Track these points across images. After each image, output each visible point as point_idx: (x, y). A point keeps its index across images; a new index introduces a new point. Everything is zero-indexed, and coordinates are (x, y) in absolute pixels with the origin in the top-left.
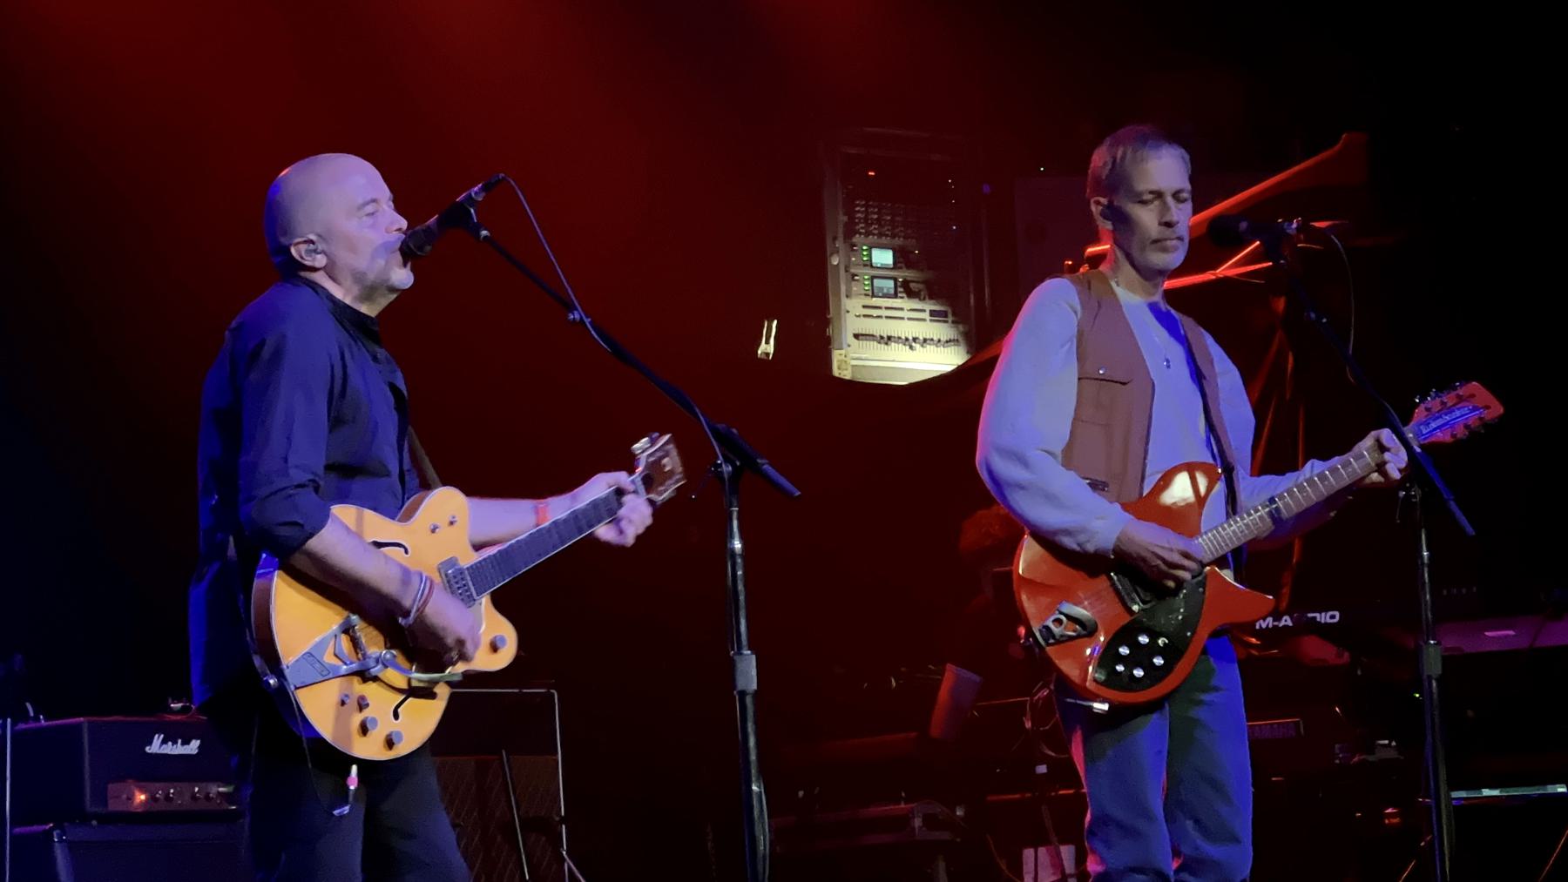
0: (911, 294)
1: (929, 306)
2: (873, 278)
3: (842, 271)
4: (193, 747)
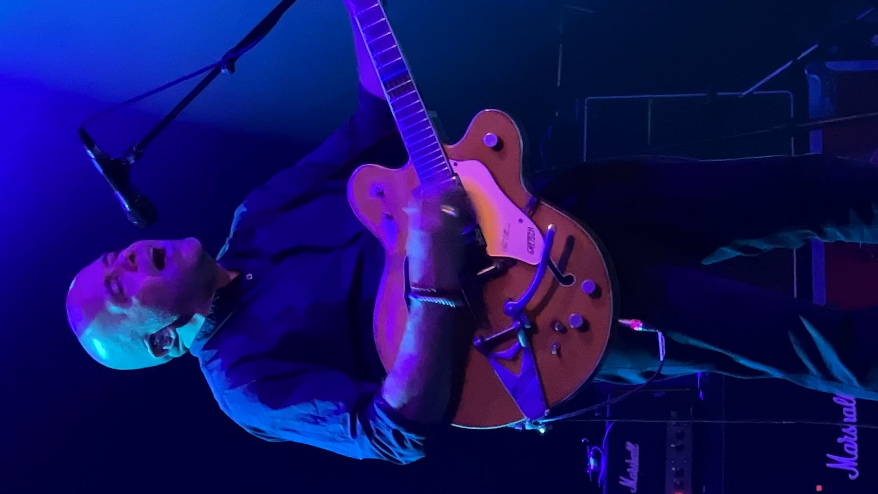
4: (630, 446)
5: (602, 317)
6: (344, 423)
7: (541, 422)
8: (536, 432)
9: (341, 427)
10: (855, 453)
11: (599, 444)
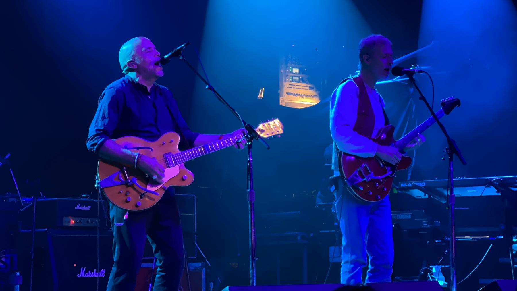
0: (304, 82)
1: (309, 85)
2: (293, 76)
3: (284, 73)
4: (89, 207)
5: (130, 207)
6: (101, 127)
7: (99, 185)
8: (95, 183)
9: (100, 125)
10: (86, 276)
11: (91, 198)
